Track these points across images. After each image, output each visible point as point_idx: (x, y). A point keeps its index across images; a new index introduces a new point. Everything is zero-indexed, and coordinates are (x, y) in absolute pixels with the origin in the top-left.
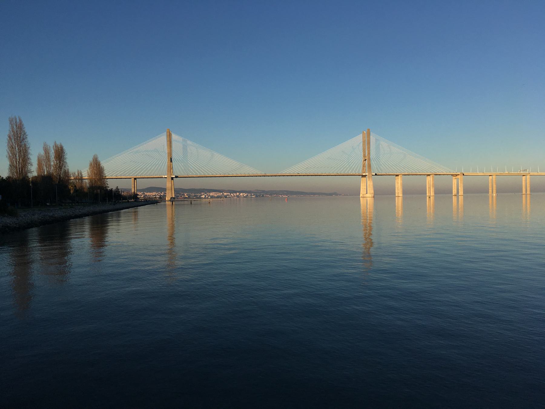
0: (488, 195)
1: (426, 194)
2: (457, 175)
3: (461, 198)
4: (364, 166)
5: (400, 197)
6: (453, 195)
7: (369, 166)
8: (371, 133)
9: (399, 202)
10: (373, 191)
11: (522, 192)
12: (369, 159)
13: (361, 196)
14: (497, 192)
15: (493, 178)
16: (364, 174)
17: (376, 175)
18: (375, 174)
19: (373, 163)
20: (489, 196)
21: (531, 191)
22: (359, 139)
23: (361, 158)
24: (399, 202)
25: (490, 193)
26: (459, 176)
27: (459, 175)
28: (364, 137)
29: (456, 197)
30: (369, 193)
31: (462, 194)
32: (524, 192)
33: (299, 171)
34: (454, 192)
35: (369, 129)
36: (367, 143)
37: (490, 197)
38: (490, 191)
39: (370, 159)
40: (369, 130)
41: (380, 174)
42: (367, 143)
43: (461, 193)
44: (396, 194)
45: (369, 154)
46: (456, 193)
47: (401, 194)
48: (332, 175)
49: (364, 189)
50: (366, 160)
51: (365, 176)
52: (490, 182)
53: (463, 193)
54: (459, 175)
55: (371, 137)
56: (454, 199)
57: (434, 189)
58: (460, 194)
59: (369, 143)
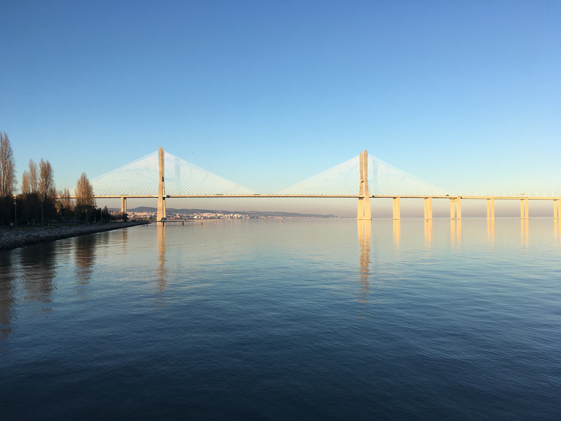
0: (486, 219)
1: (424, 217)
2: (455, 198)
3: (459, 222)
4: (361, 188)
7: (367, 188)
9: (397, 225)
12: (367, 181)
13: (358, 219)
14: (496, 216)
16: (361, 196)
17: (373, 197)
18: (373, 196)
19: (370, 185)
21: (529, 216)
22: (357, 160)
24: (397, 225)
28: (361, 159)
32: (522, 217)
33: (295, 193)
34: (452, 216)
35: (367, 151)
36: (364, 165)
39: (367, 181)
40: (366, 151)
42: (364, 165)
43: (459, 216)
45: (366, 175)
48: (328, 197)
50: (363, 182)
55: (369, 158)
56: (452, 222)
58: (457, 218)
59: (366, 165)
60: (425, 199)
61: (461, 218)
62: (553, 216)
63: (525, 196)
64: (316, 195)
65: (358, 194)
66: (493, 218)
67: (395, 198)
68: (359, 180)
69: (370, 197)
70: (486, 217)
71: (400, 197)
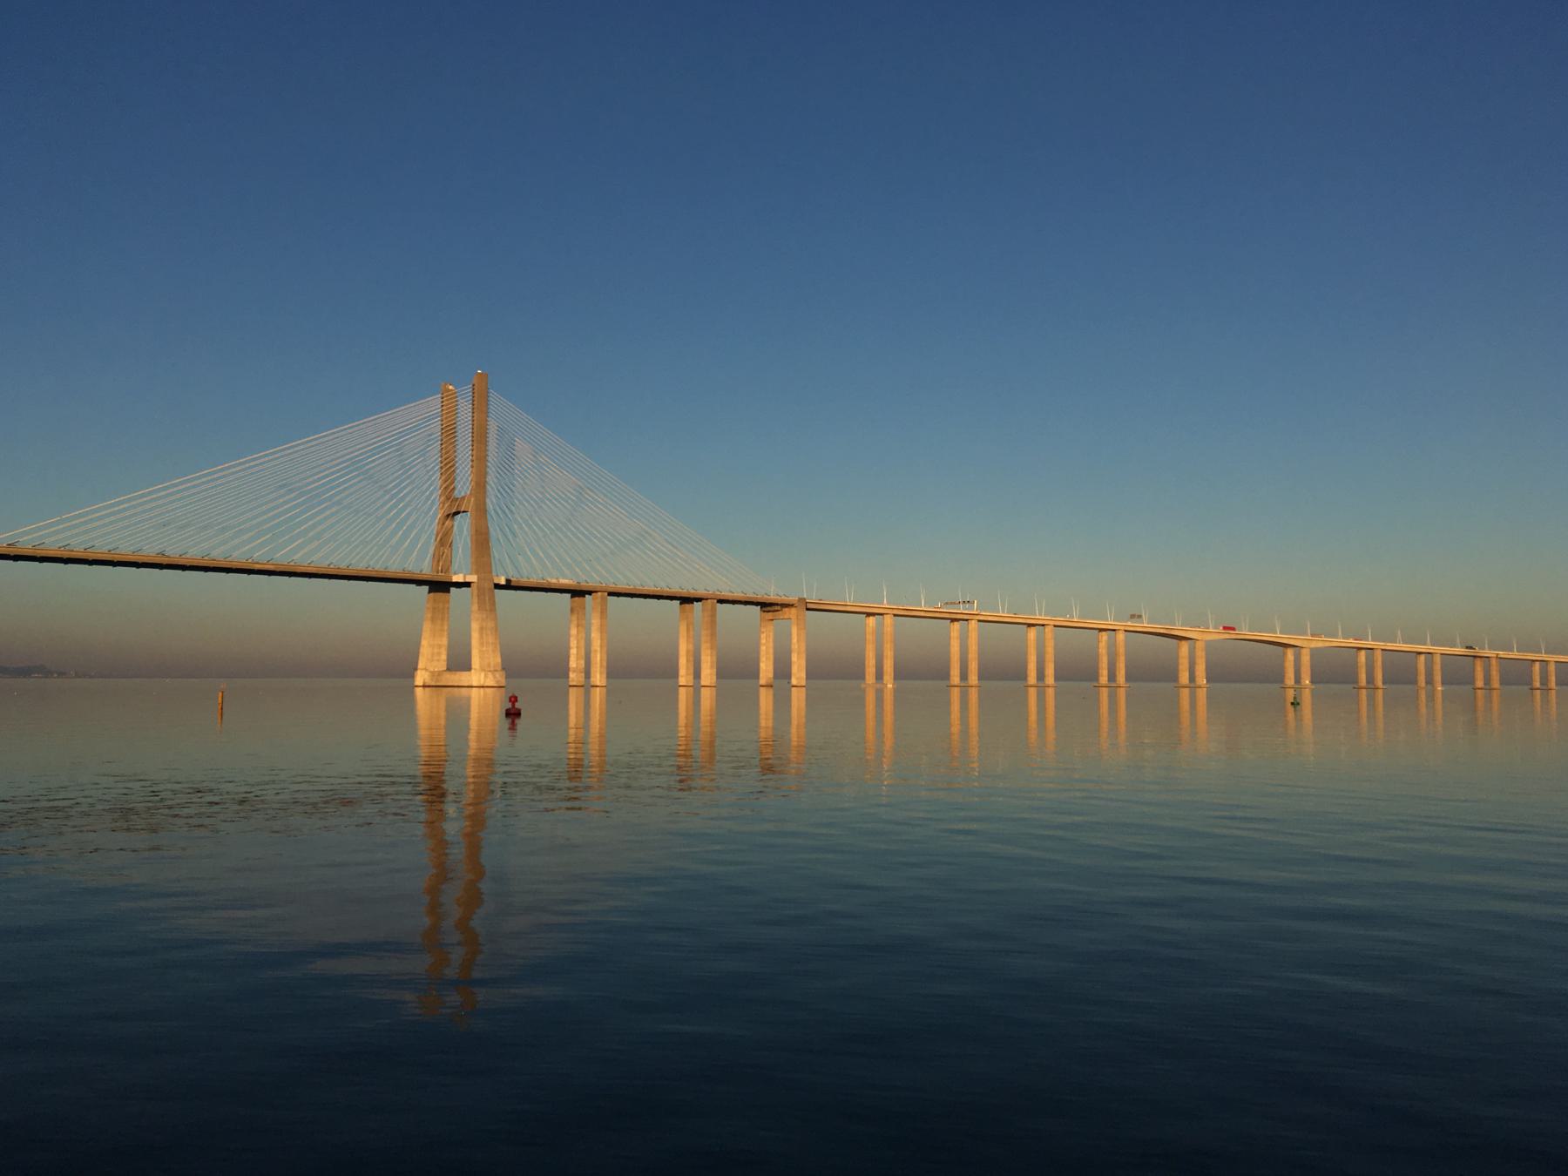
0: (863, 686)
1: (676, 675)
4: (444, 540)
5: (598, 689)
7: (482, 542)
8: (493, 395)
10: (499, 660)
11: (1097, 680)
13: (419, 680)
14: (898, 676)
15: (880, 626)
16: (441, 577)
17: (509, 586)
18: (508, 581)
20: (864, 691)
23: (433, 503)
25: (870, 678)
26: (793, 610)
27: (792, 605)
29: (771, 691)
30: (482, 669)
31: (804, 683)
37: (870, 698)
41: (524, 581)
44: (572, 675)
46: (771, 675)
47: (601, 673)
49: (436, 651)
51: (440, 586)
52: (870, 637)
53: (807, 678)
54: (792, 605)
57: (715, 659)
58: (794, 681)
60: (681, 604)
61: (804, 683)
62: (1023, 676)
65: (426, 569)
67: (578, 593)
70: (862, 676)
71: (611, 594)
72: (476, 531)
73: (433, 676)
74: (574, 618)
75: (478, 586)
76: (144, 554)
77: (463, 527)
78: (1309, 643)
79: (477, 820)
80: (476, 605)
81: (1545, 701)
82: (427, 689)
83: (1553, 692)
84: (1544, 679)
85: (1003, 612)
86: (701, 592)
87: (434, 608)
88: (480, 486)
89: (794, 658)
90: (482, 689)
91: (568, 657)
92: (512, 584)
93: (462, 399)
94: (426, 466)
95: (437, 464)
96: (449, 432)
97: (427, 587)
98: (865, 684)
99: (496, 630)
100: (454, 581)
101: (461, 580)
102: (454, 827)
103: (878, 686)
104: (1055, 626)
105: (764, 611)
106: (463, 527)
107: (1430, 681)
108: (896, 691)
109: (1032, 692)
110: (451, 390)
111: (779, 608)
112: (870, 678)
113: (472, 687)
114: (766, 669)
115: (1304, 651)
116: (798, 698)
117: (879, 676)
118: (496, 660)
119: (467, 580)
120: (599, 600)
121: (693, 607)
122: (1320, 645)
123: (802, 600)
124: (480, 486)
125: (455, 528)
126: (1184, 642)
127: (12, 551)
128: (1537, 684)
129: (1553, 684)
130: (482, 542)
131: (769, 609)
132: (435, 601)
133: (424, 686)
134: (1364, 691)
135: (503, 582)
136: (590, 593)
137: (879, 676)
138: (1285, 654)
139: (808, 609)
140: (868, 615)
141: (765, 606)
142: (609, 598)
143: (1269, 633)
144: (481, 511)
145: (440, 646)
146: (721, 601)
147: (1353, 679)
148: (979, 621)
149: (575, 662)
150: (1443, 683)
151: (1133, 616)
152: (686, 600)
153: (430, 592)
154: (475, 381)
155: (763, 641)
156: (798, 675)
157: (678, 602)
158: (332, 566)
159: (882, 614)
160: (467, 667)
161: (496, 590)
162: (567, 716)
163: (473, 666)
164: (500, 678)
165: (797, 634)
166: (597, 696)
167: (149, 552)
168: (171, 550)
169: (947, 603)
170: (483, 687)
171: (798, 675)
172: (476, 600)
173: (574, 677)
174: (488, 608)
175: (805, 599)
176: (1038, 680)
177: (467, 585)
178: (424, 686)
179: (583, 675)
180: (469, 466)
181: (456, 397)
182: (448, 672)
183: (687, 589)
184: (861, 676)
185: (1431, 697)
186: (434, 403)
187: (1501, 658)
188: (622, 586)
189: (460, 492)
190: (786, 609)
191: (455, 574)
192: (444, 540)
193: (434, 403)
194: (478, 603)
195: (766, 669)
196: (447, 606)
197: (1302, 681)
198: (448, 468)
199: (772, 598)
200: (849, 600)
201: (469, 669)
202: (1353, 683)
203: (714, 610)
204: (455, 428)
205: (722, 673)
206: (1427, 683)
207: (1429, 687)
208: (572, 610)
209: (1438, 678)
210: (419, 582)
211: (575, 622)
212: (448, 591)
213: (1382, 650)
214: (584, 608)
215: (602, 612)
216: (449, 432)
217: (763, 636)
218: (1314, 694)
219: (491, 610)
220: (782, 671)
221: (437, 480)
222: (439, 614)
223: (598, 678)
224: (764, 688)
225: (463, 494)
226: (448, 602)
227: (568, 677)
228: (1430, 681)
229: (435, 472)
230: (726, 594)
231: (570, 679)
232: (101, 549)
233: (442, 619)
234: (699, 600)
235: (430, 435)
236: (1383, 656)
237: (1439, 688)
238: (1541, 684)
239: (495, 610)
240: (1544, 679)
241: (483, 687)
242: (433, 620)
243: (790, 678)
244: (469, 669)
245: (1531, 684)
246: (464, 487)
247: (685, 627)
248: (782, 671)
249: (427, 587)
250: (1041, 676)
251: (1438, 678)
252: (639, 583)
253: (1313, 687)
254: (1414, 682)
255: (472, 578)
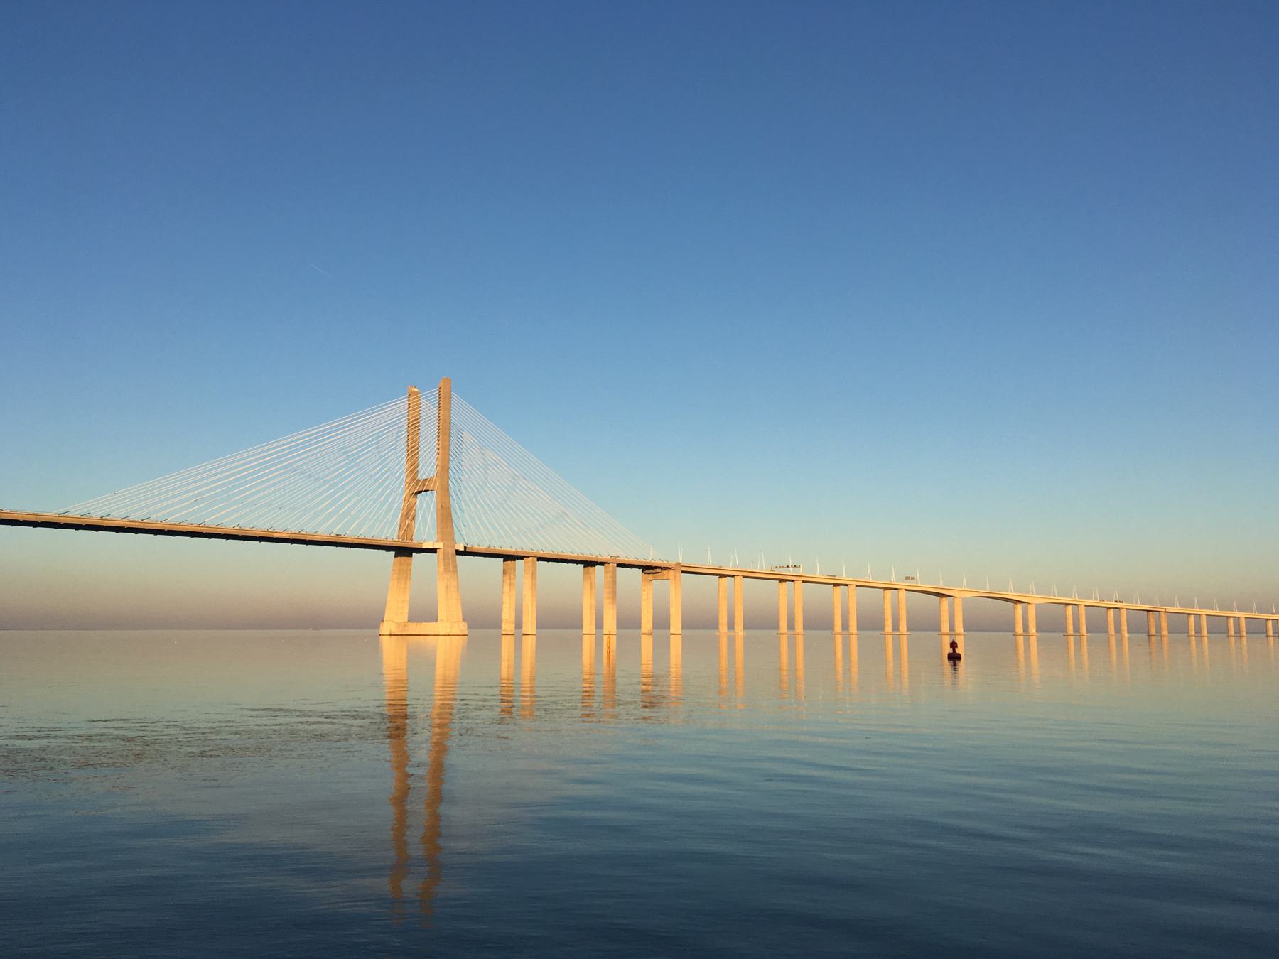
0: (718, 634)
1: (581, 627)
4: (409, 515)
5: (529, 636)
6: (643, 630)
7: (445, 517)
8: (454, 395)
13: (386, 628)
14: (746, 627)
18: (465, 547)
25: (723, 628)
26: (671, 572)
27: (670, 568)
28: (414, 409)
29: (650, 638)
31: (680, 631)
38: (723, 620)
40: (448, 381)
44: (503, 625)
51: (404, 552)
53: (683, 628)
54: (670, 568)
58: (672, 631)
60: (584, 567)
63: (799, 572)
64: (265, 528)
65: (392, 535)
66: (740, 630)
67: (509, 558)
68: (401, 489)
69: (458, 552)
70: (716, 627)
72: (442, 506)
73: (399, 627)
74: (507, 577)
75: (444, 553)
76: (70, 515)
77: (427, 506)
78: (1035, 599)
79: (440, 748)
80: (443, 567)
81: (1200, 643)
82: (393, 637)
83: (1206, 638)
84: (1198, 631)
85: (1033, 593)
86: (604, 556)
87: (400, 570)
88: (444, 469)
89: (672, 611)
90: (448, 637)
91: (501, 610)
92: (467, 550)
93: (424, 399)
94: (380, 452)
95: (403, 453)
96: (414, 426)
97: (394, 553)
98: (719, 632)
99: (458, 589)
100: (424, 547)
101: (431, 547)
102: (421, 753)
103: (732, 633)
104: (857, 586)
105: (645, 573)
106: (427, 506)
107: (1118, 630)
108: (745, 637)
109: (839, 639)
110: (417, 393)
111: (660, 570)
112: (723, 628)
113: (438, 635)
114: (647, 624)
115: (1122, 610)
116: (676, 644)
117: (731, 626)
118: (458, 614)
119: (435, 547)
120: (531, 564)
121: (595, 570)
122: (1042, 601)
123: (678, 564)
124: (444, 469)
125: (417, 503)
126: (944, 599)
127: (203, 530)
128: (1193, 633)
129: (1205, 632)
130: (445, 517)
131: (651, 571)
132: (401, 564)
133: (391, 635)
134: (1072, 638)
135: (462, 549)
136: (522, 558)
137: (731, 626)
138: (1015, 609)
139: (683, 572)
140: (836, 585)
141: (646, 568)
142: (618, 568)
143: (1062, 597)
144: (445, 490)
145: (403, 601)
146: (621, 565)
147: (1063, 629)
148: (803, 582)
149: (508, 615)
150: (1128, 632)
151: (907, 578)
152: (589, 564)
153: (395, 556)
154: (441, 384)
155: (644, 597)
156: (676, 625)
157: (583, 565)
158: (332, 535)
159: (733, 576)
160: (434, 618)
161: (458, 556)
162: (500, 658)
163: (439, 619)
164: (462, 628)
165: (674, 591)
166: (529, 644)
167: (323, 532)
168: (75, 511)
169: (776, 567)
170: (449, 635)
171: (676, 625)
172: (442, 563)
173: (508, 627)
174: (451, 569)
175: (680, 564)
176: (842, 629)
177: (434, 551)
178: (391, 635)
179: (514, 625)
180: (436, 453)
181: (420, 397)
182: (409, 623)
183: (507, 548)
184: (715, 626)
185: (1120, 642)
186: (401, 406)
187: (1168, 612)
188: (548, 552)
189: (422, 476)
190: (665, 572)
191: (424, 541)
192: (409, 515)
193: (402, 405)
194: (444, 565)
195: (647, 624)
196: (409, 568)
197: (1030, 629)
198: (413, 452)
199: (657, 562)
200: (710, 562)
201: (434, 618)
202: (1063, 632)
203: (534, 566)
204: (419, 422)
205: (620, 625)
206: (1116, 632)
207: (1119, 634)
208: (505, 572)
209: (1125, 628)
210: (387, 548)
211: (508, 582)
212: (411, 556)
213: (1085, 606)
214: (515, 570)
215: (533, 574)
216: (414, 426)
217: (644, 593)
218: (1038, 640)
219: (453, 572)
220: (661, 623)
221: (403, 465)
222: (404, 574)
223: (529, 626)
224: (646, 636)
225: (431, 475)
226: (411, 565)
227: (500, 628)
228: (1118, 630)
229: (403, 458)
230: (624, 559)
231: (503, 629)
232: (154, 520)
233: (406, 579)
234: (602, 564)
235: (401, 427)
236: (1086, 610)
237: (1126, 635)
238: (1235, 633)
239: (456, 571)
240: (1198, 631)
241: (449, 635)
242: (399, 579)
243: (669, 628)
244: (436, 621)
245: (1189, 633)
246: (428, 468)
247: (589, 585)
248: (661, 623)
249: (394, 553)
250: (845, 626)
251: (1125, 628)
252: (588, 552)
253: (1038, 634)
254: (1106, 631)
255: (438, 545)
